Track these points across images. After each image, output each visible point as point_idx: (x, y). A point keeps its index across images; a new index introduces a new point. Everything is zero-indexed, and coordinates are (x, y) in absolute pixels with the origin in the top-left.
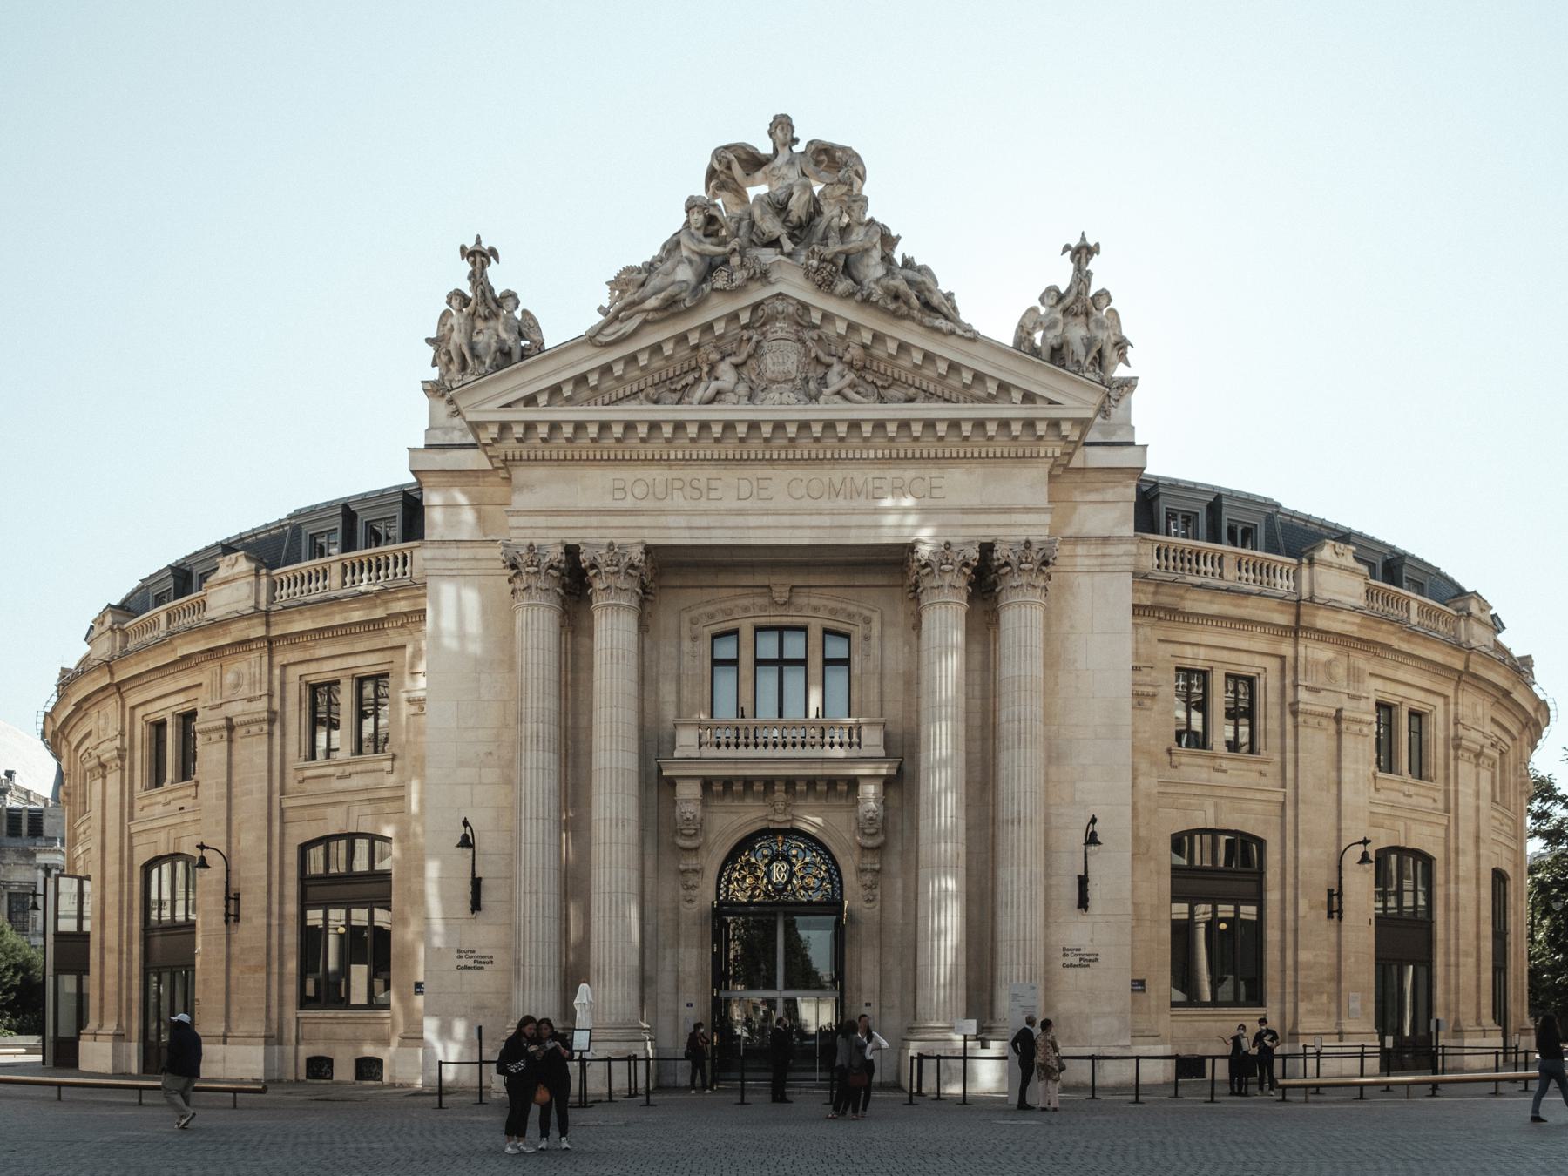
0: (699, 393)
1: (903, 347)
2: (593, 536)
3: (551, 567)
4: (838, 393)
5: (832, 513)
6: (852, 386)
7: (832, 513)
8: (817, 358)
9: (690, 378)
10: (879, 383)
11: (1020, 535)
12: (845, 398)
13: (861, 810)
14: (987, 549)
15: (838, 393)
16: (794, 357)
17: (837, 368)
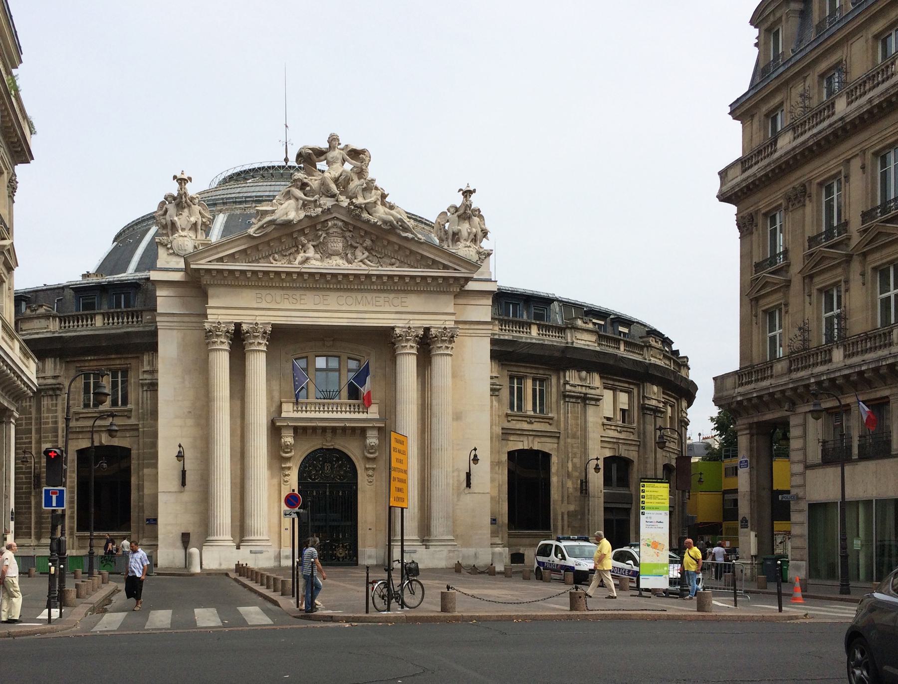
0: (300, 257)
2: (247, 319)
4: (361, 261)
9: (293, 250)
13: (368, 441)
14: (427, 330)
15: (361, 261)
16: (341, 244)
17: (360, 248)
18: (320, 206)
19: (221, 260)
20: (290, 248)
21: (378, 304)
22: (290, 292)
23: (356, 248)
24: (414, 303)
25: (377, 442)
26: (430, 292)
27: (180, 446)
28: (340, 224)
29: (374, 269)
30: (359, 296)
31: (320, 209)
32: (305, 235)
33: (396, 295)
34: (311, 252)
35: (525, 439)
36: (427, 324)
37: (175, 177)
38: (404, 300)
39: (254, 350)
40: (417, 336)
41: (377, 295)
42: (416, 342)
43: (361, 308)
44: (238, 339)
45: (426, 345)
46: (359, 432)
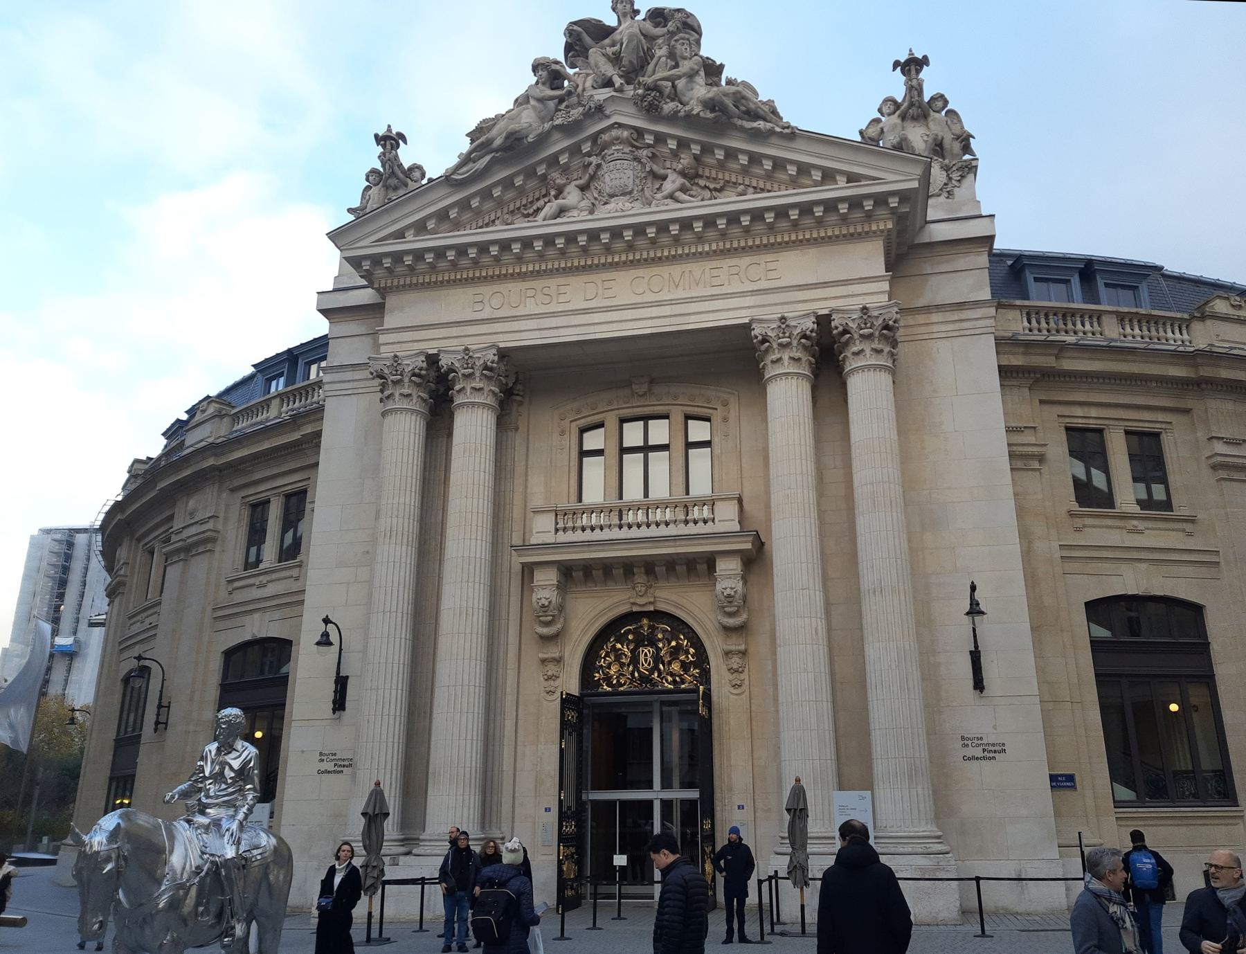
1: (731, 154)
3: (414, 375)
4: (671, 196)
5: (671, 303)
6: (683, 189)
7: (671, 303)
8: (651, 172)
9: (542, 202)
10: (712, 186)
11: (860, 302)
12: (678, 201)
15: (671, 196)
17: (672, 176)
18: (579, 104)
19: (400, 235)
20: (538, 199)
21: (716, 281)
22: (538, 284)
23: (664, 178)
24: (795, 267)
25: (739, 586)
26: (829, 240)
27: (327, 621)
28: (626, 134)
29: (696, 206)
30: (676, 270)
31: (581, 109)
32: (565, 169)
33: (755, 259)
34: (572, 196)
35: (1125, 569)
36: (823, 308)
37: (376, 136)
38: (771, 266)
39: (462, 405)
40: (805, 336)
41: (714, 264)
42: (805, 348)
43: (681, 294)
44: (437, 391)
45: (826, 354)
46: (699, 567)
